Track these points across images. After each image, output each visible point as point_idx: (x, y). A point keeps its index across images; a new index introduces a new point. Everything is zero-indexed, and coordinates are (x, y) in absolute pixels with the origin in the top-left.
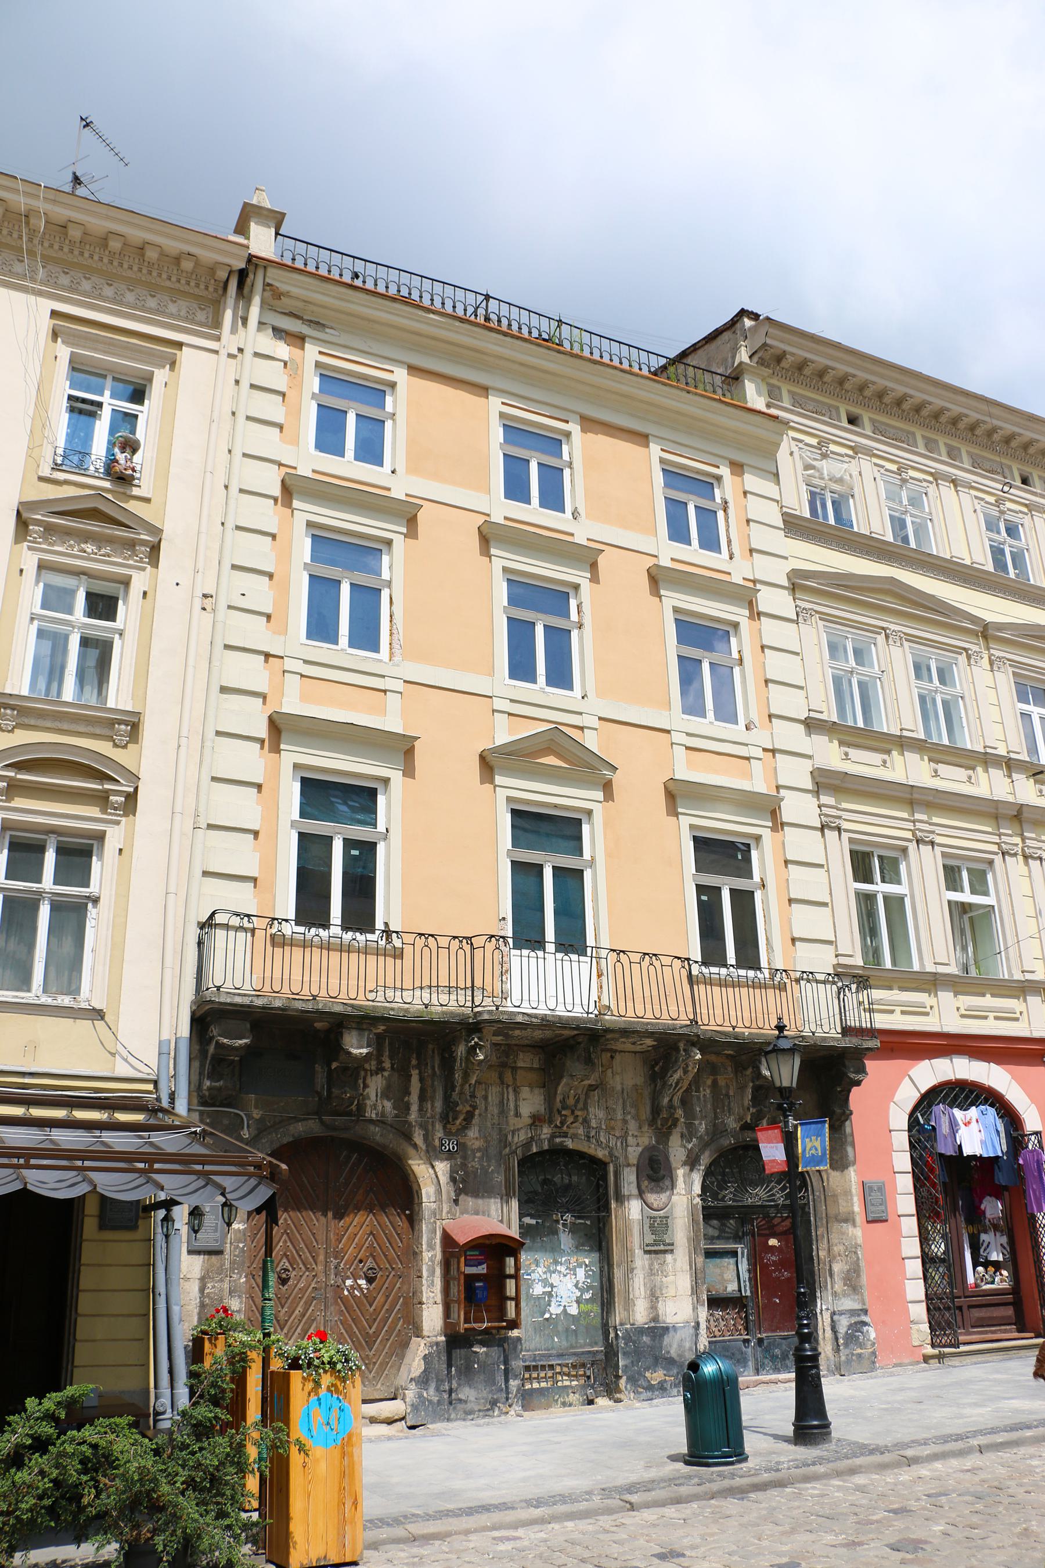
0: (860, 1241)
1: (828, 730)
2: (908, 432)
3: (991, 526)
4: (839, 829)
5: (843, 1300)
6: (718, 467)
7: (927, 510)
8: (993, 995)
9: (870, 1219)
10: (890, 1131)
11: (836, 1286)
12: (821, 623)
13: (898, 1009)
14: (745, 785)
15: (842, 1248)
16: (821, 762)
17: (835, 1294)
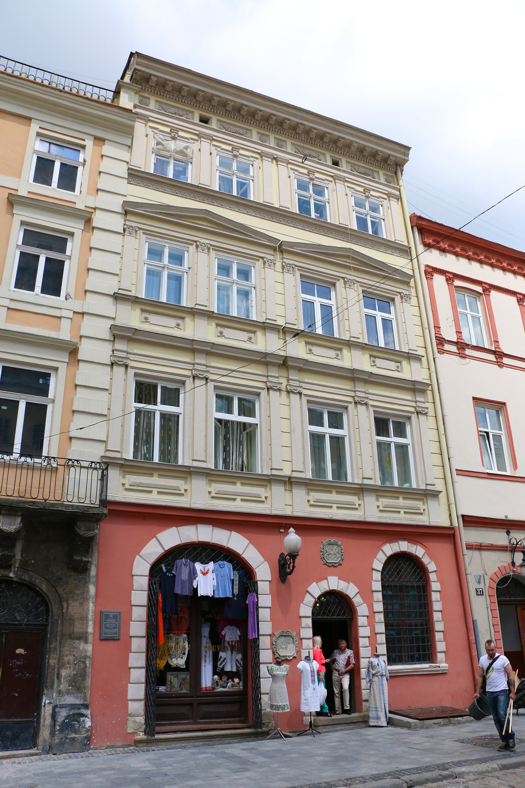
0: (89, 653)
1: (132, 302)
2: (248, 130)
3: (302, 186)
4: (126, 366)
5: (66, 697)
6: (84, 140)
7: (251, 174)
8: (242, 484)
9: (103, 638)
10: (133, 576)
11: (62, 686)
12: (143, 237)
13: (155, 491)
14: (53, 334)
15: (71, 658)
16: (119, 322)
17: (60, 692)
